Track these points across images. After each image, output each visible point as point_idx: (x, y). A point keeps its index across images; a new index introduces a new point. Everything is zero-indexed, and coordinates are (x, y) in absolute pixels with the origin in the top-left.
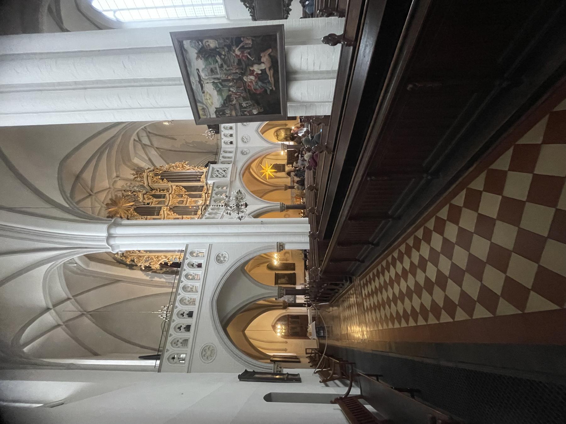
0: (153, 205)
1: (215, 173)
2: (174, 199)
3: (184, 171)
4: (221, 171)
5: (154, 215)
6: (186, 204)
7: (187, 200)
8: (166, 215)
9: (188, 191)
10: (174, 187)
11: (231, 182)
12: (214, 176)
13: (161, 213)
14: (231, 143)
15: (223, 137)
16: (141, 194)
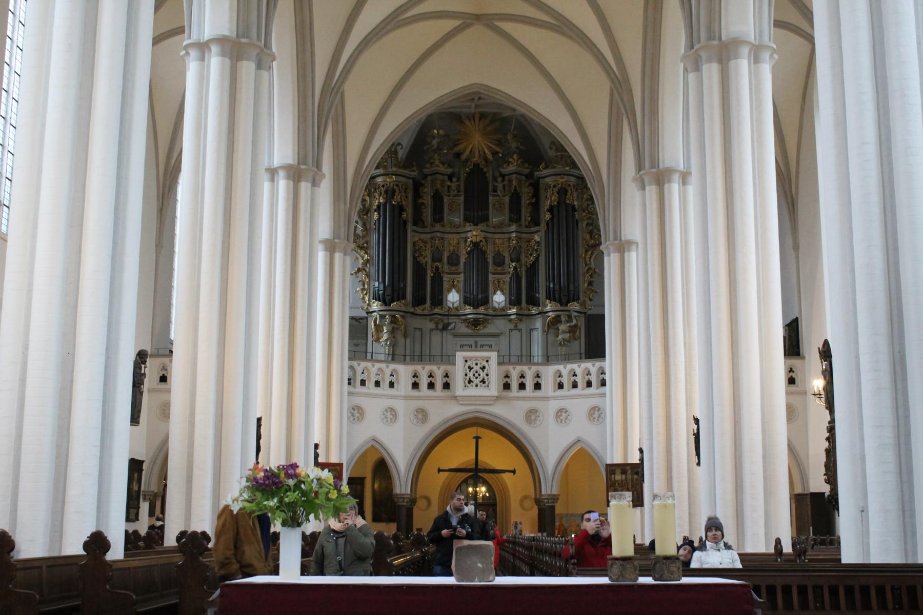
0: (491, 198)
1: (477, 364)
2: (506, 244)
3: (581, 251)
4: (483, 375)
5: (465, 210)
6: (494, 274)
7: (504, 274)
8: (463, 235)
9: (527, 271)
10: (537, 238)
11: (455, 398)
12: (469, 363)
13: (468, 224)
14: (561, 386)
15: (570, 366)
16: (514, 168)
